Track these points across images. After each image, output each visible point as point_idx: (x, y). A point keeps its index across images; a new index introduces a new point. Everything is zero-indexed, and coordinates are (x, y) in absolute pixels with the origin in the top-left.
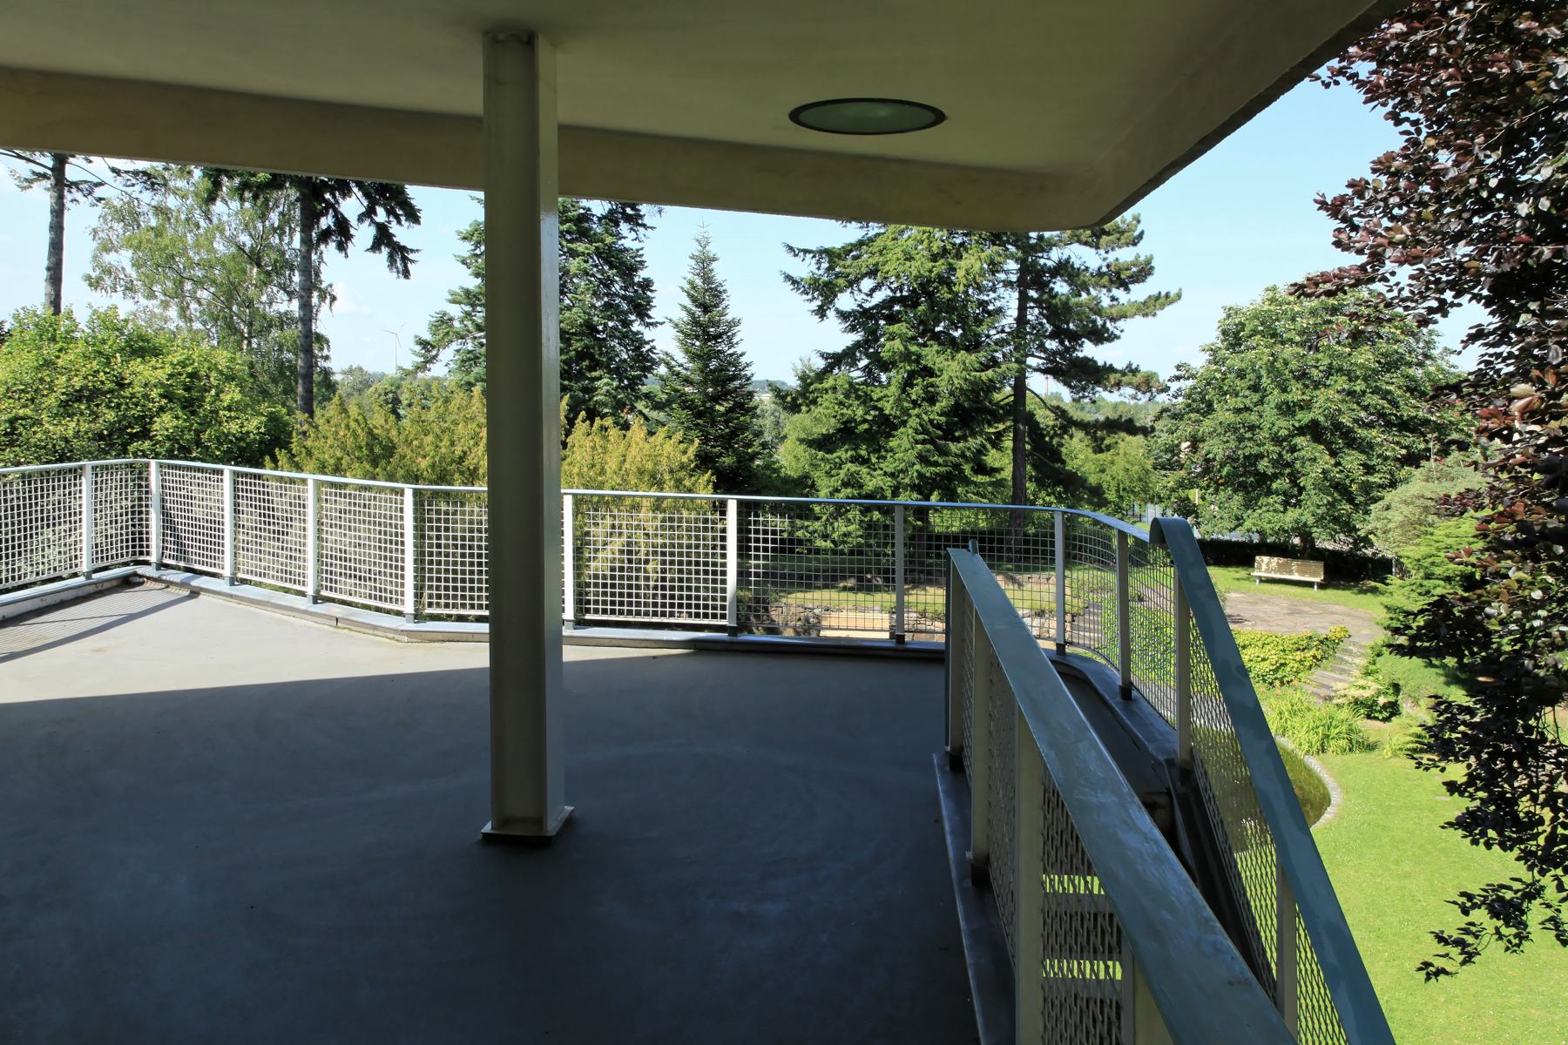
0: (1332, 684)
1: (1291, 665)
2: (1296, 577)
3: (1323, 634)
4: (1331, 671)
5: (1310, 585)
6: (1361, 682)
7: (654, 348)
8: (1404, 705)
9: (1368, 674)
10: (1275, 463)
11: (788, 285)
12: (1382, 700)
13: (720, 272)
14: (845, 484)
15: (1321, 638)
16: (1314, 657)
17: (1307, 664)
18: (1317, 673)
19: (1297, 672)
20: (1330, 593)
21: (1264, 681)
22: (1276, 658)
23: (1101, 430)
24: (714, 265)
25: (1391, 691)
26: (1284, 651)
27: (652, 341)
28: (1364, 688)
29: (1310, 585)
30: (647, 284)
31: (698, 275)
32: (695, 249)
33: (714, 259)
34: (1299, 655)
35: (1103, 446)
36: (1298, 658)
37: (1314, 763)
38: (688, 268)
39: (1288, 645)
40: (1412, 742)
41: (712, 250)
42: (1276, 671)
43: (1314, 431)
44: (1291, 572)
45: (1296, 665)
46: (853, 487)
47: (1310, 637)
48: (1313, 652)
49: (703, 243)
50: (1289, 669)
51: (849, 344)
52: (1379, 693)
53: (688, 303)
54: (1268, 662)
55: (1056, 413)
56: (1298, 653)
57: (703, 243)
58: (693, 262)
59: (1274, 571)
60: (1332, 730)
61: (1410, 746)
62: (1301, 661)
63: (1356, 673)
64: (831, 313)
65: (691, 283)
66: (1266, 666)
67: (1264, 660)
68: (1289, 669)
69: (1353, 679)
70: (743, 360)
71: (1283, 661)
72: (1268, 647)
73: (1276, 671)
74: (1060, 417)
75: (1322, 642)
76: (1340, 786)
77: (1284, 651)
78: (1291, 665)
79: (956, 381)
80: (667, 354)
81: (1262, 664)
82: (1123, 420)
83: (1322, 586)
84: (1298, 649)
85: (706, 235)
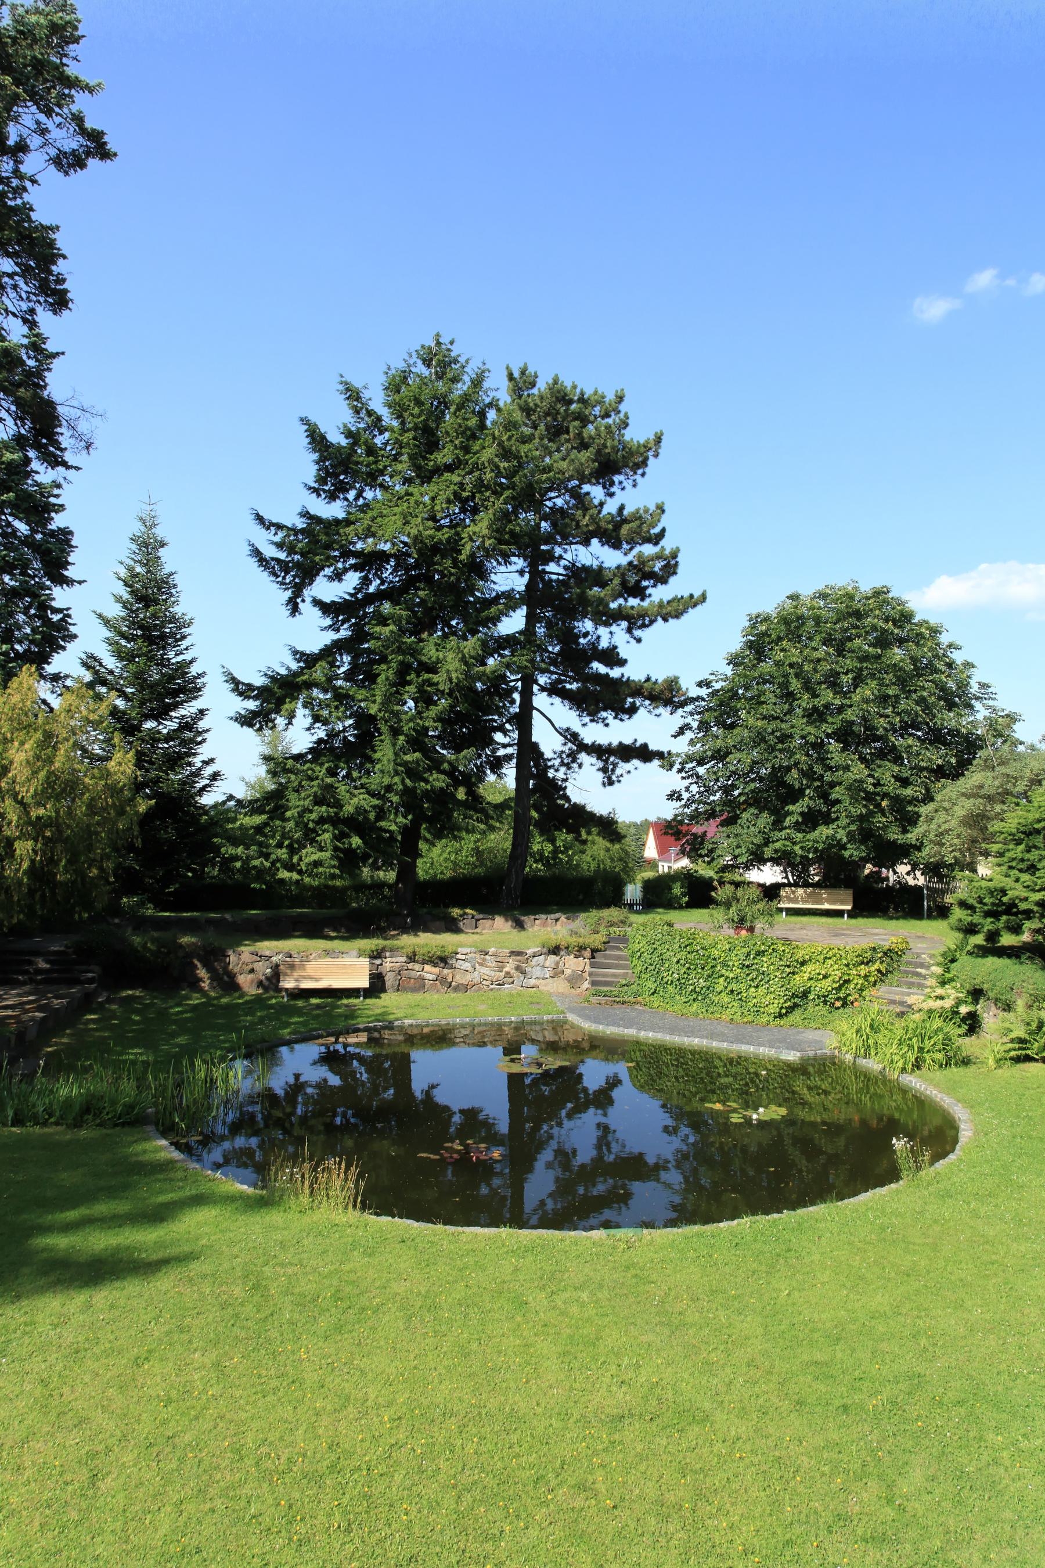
0: (906, 998)
1: (855, 982)
2: (826, 906)
3: (886, 945)
4: (898, 986)
5: (839, 914)
6: (940, 991)
7: (69, 616)
8: (985, 1015)
9: (943, 983)
10: (804, 774)
11: (253, 562)
12: (964, 1010)
13: (169, 560)
14: (318, 801)
15: (885, 949)
16: (879, 971)
17: (872, 979)
18: (882, 990)
19: (862, 990)
20: (861, 922)
21: (825, 1002)
22: (839, 973)
23: (615, 756)
24: (162, 552)
25: (970, 999)
26: (847, 965)
27: (68, 609)
28: (942, 998)
29: (839, 914)
30: (64, 537)
31: (140, 562)
32: (138, 528)
33: (163, 545)
34: (863, 970)
35: (614, 778)
36: (862, 973)
37: (914, 1081)
38: (127, 553)
39: (851, 958)
40: (1015, 1050)
41: (160, 532)
42: (839, 989)
43: (845, 736)
44: (820, 901)
45: (860, 982)
46: (328, 805)
47: (874, 949)
48: (877, 965)
49: (149, 523)
50: (852, 986)
51: (328, 642)
52: (959, 1002)
53: (124, 593)
54: (830, 979)
55: (565, 737)
56: (863, 966)
57: (149, 523)
58: (134, 547)
59: (804, 901)
60: (926, 1042)
61: (1013, 1053)
62: (866, 976)
63: (931, 982)
64: (306, 607)
65: (130, 569)
66: (827, 985)
67: (825, 977)
68: (852, 986)
69: (929, 990)
70: (194, 670)
71: (846, 977)
72: (830, 962)
73: (839, 989)
74: (570, 741)
75: (885, 954)
76: (959, 1101)
77: (847, 965)
78: (855, 982)
79: (454, 675)
80: (95, 659)
81: (823, 982)
82: (638, 745)
83: (852, 915)
84: (863, 963)
85: (153, 513)
